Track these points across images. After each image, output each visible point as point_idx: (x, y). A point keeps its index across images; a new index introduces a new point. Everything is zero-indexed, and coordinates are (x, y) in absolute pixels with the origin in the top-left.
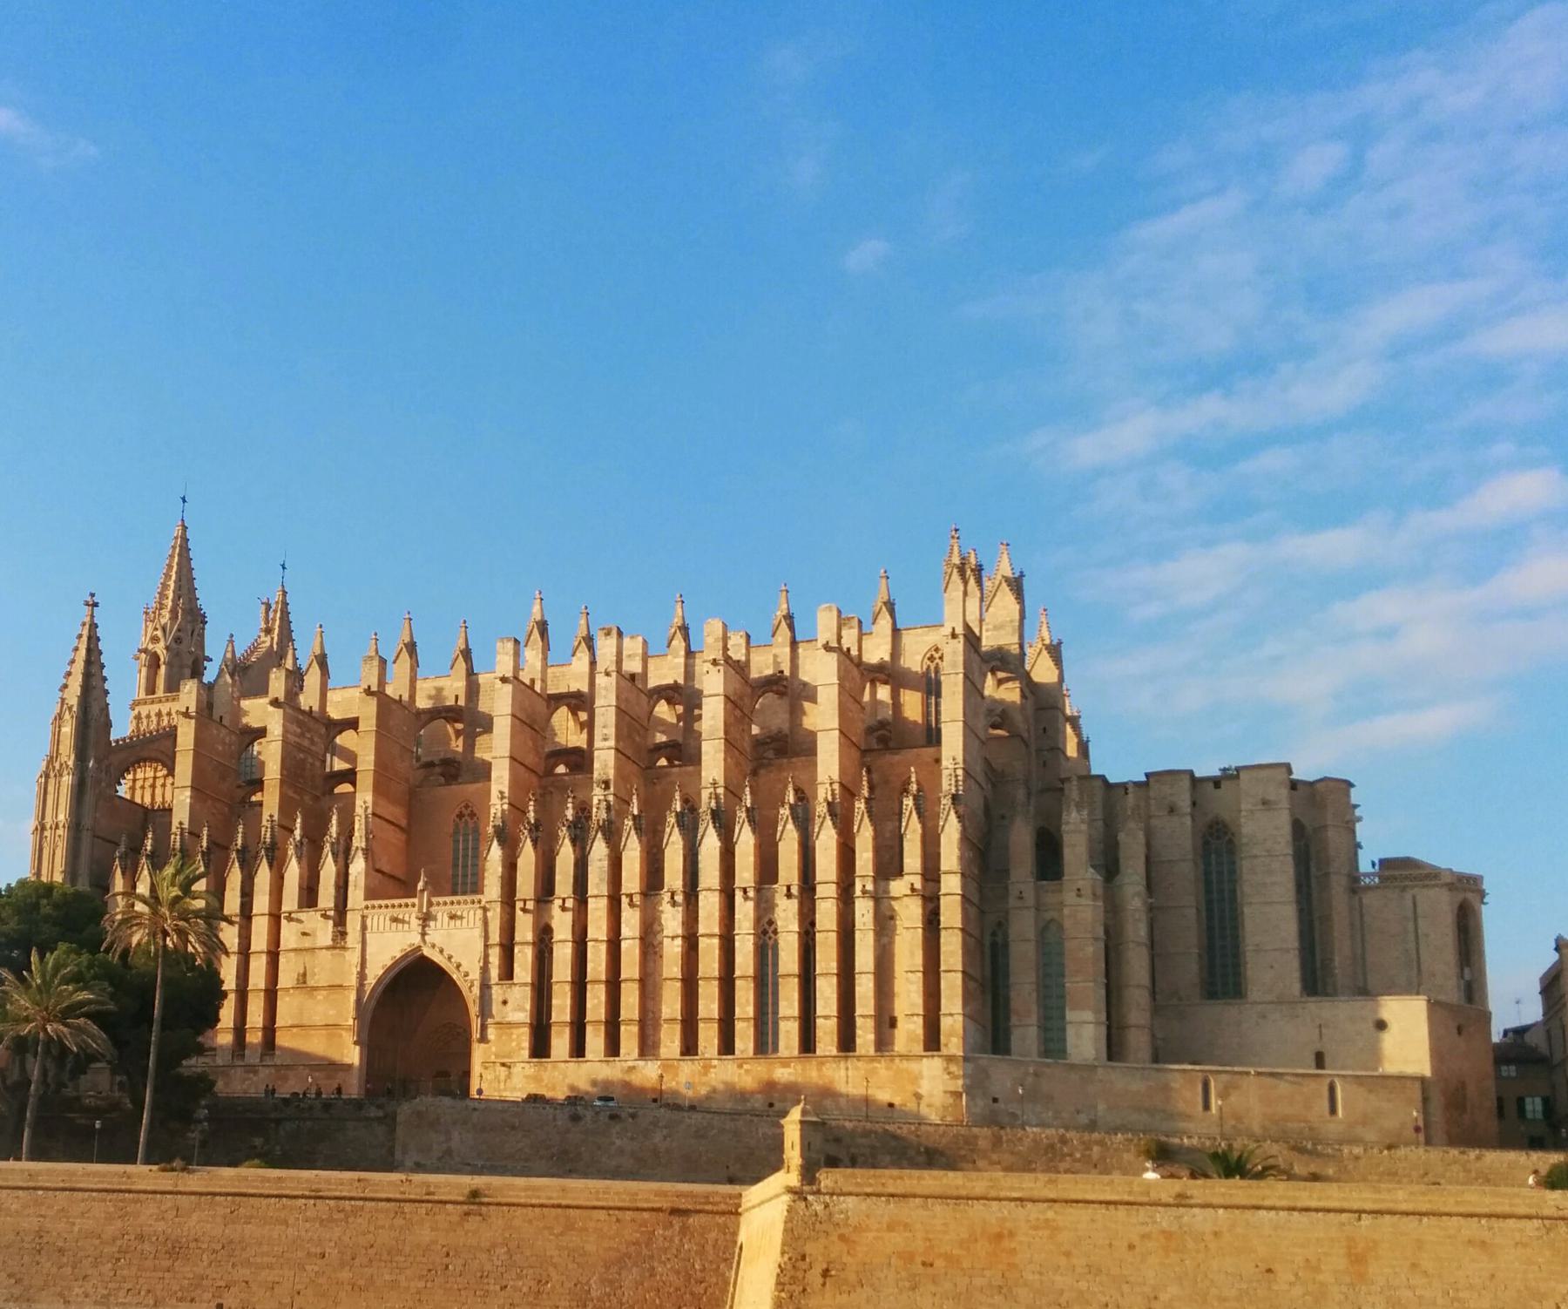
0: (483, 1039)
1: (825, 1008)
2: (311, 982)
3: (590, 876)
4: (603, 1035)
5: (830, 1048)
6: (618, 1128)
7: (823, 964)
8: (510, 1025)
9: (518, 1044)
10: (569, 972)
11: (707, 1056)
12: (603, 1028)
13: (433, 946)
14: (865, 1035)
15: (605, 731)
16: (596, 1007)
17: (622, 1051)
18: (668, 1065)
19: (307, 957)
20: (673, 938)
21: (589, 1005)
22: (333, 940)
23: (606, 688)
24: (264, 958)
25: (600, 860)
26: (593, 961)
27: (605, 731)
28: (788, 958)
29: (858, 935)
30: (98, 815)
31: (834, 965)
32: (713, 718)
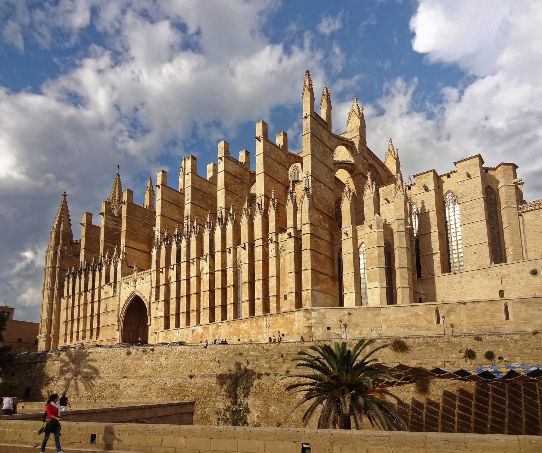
1: (258, 295)
3: (181, 255)
5: (260, 312)
6: (146, 356)
11: (218, 321)
13: (138, 291)
14: (273, 305)
16: (183, 306)
18: (205, 328)
20: (207, 274)
21: (181, 306)
24: (97, 302)
26: (182, 288)
28: (245, 276)
29: (270, 260)
30: (63, 263)
31: (261, 275)
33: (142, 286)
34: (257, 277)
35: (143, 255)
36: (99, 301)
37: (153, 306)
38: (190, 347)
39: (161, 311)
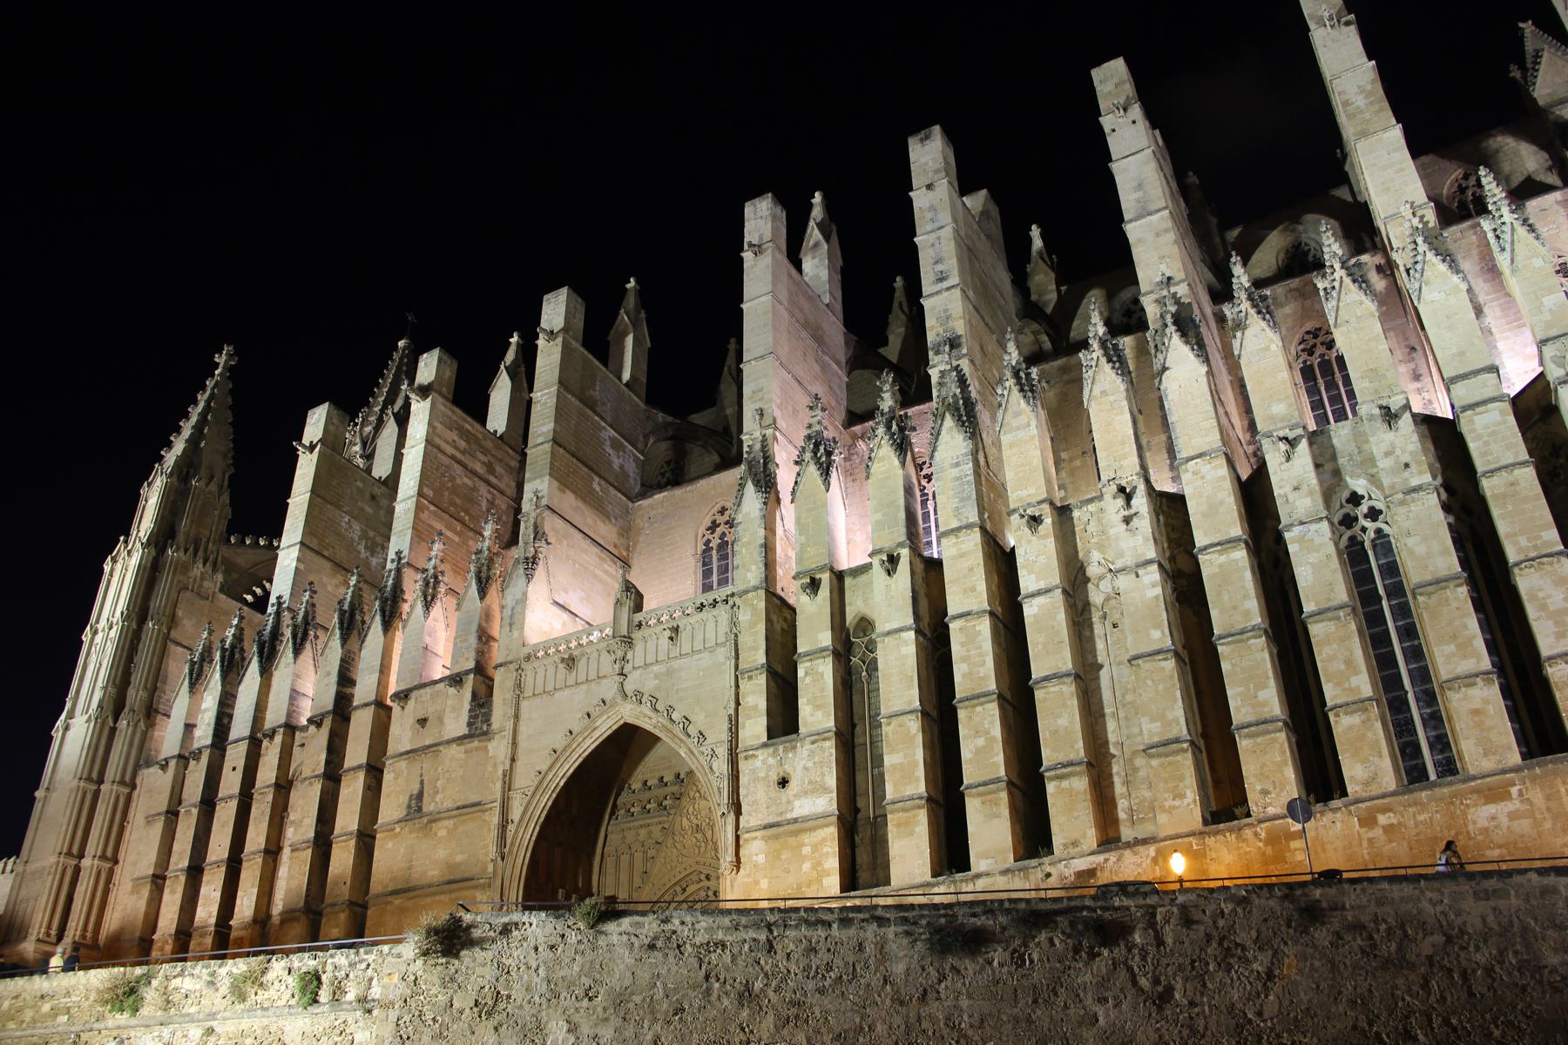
0: (738, 863)
2: (428, 806)
4: (1006, 812)
7: (1523, 541)
8: (800, 826)
9: (817, 864)
10: (916, 692)
12: (1004, 796)
15: (940, 267)
16: (978, 752)
17: (1058, 840)
19: (426, 762)
21: (966, 753)
22: (469, 724)
23: (932, 208)
24: (361, 776)
25: (957, 465)
27: (940, 267)
32: (1140, 186)
33: (670, 673)
34: (1520, 550)
35: (606, 566)
36: (375, 771)
37: (759, 767)
38: (1449, 887)
39: (818, 789)
